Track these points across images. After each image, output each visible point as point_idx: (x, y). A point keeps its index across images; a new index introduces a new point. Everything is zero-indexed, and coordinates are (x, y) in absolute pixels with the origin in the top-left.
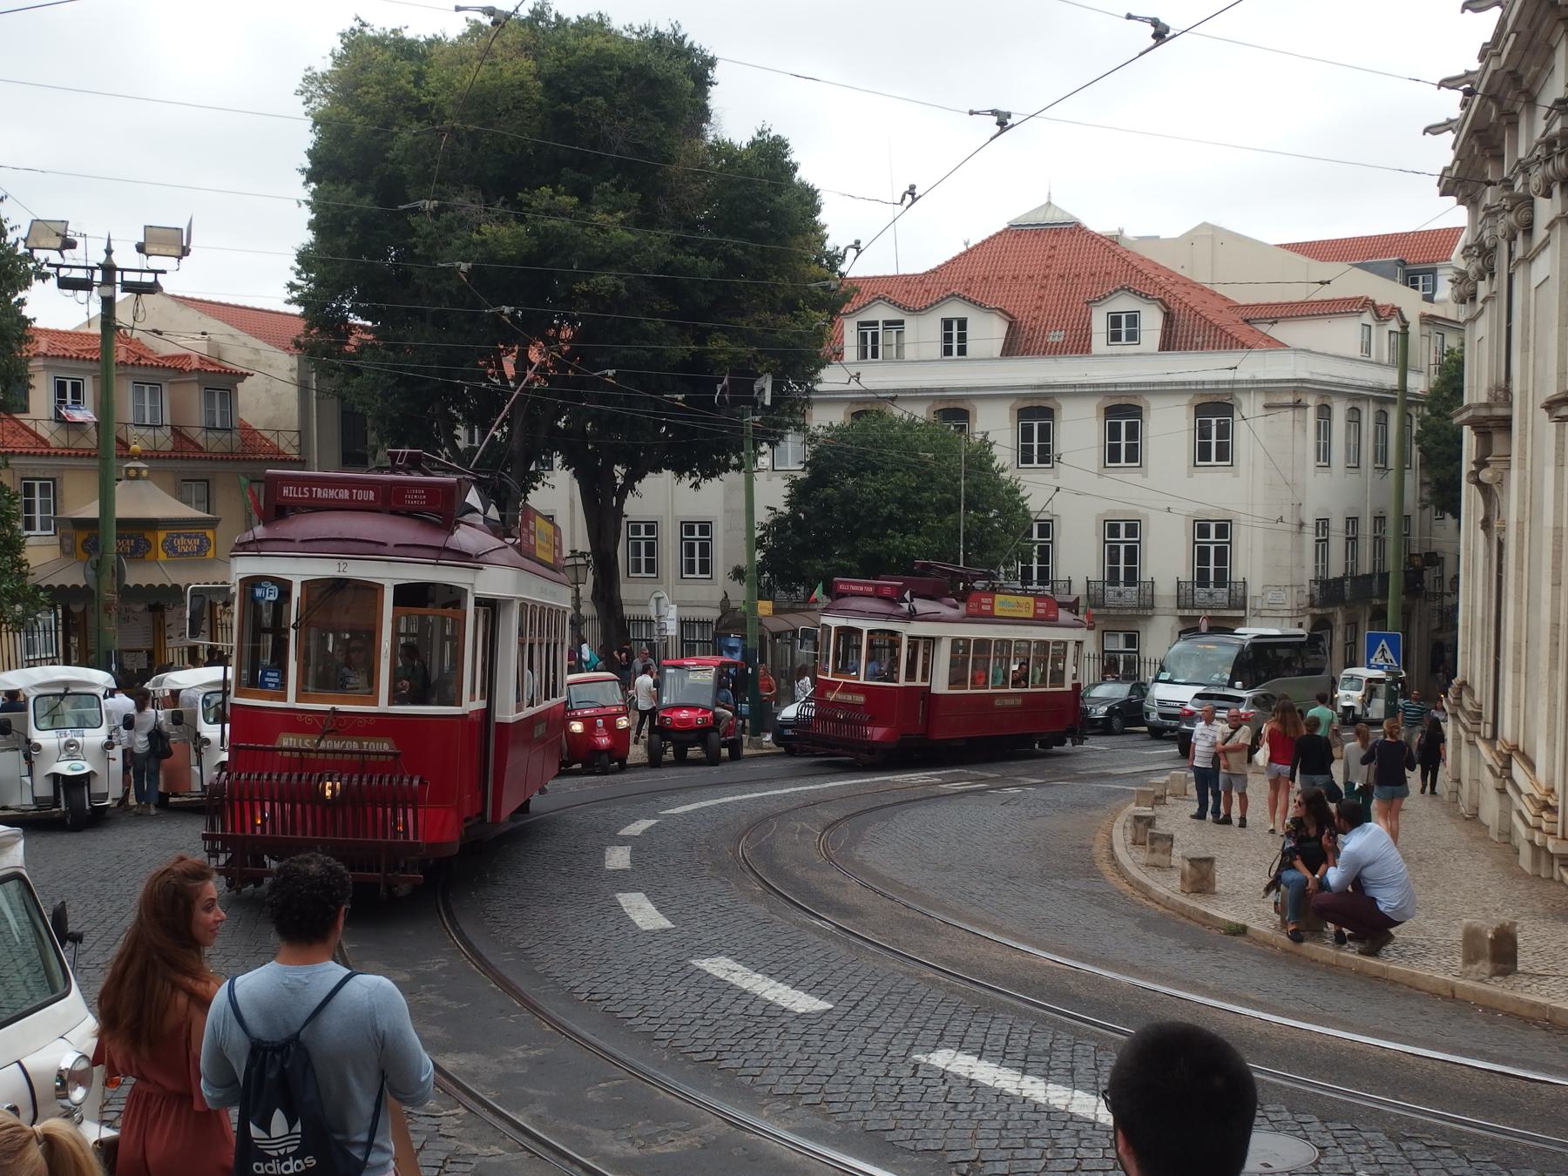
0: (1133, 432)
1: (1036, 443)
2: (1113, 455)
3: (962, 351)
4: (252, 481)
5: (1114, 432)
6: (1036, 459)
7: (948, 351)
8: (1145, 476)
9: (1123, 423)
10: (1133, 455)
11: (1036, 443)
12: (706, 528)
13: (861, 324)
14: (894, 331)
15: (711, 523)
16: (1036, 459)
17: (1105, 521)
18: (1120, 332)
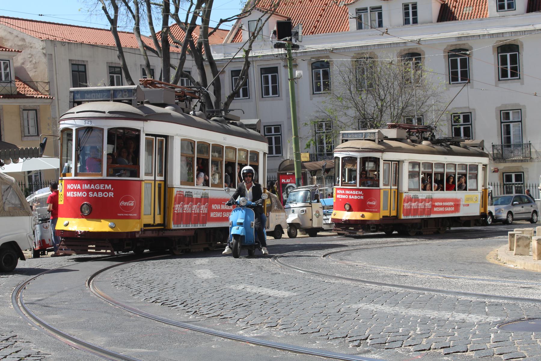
0: (514, 60)
1: (459, 70)
2: (504, 74)
3: (415, 21)
4: (24, 110)
5: (504, 61)
6: (460, 79)
7: (407, 22)
8: (522, 84)
9: (508, 55)
10: (515, 73)
11: (459, 70)
12: (278, 129)
13: (358, 10)
14: (377, 13)
15: (280, 125)
16: (460, 79)
17: (501, 111)
18: (504, 4)
